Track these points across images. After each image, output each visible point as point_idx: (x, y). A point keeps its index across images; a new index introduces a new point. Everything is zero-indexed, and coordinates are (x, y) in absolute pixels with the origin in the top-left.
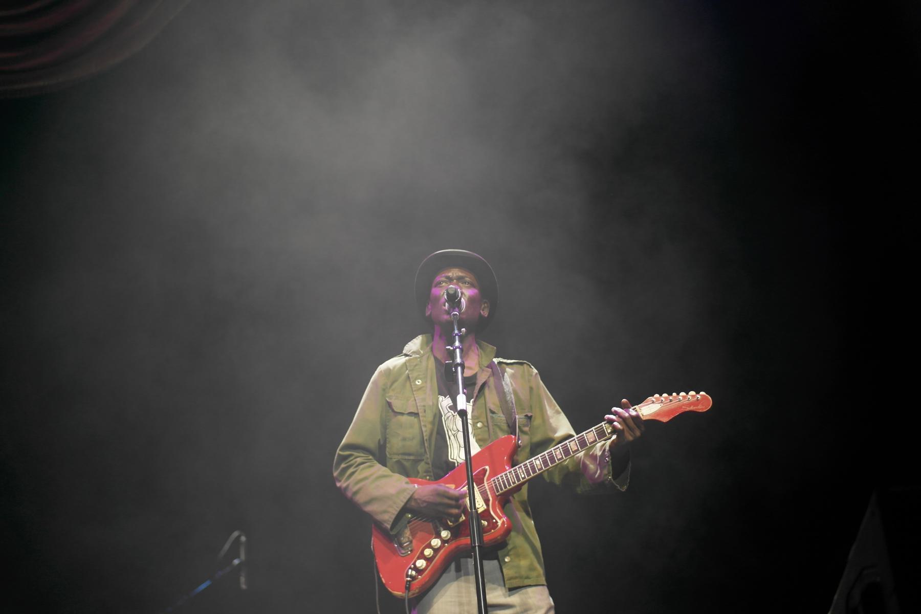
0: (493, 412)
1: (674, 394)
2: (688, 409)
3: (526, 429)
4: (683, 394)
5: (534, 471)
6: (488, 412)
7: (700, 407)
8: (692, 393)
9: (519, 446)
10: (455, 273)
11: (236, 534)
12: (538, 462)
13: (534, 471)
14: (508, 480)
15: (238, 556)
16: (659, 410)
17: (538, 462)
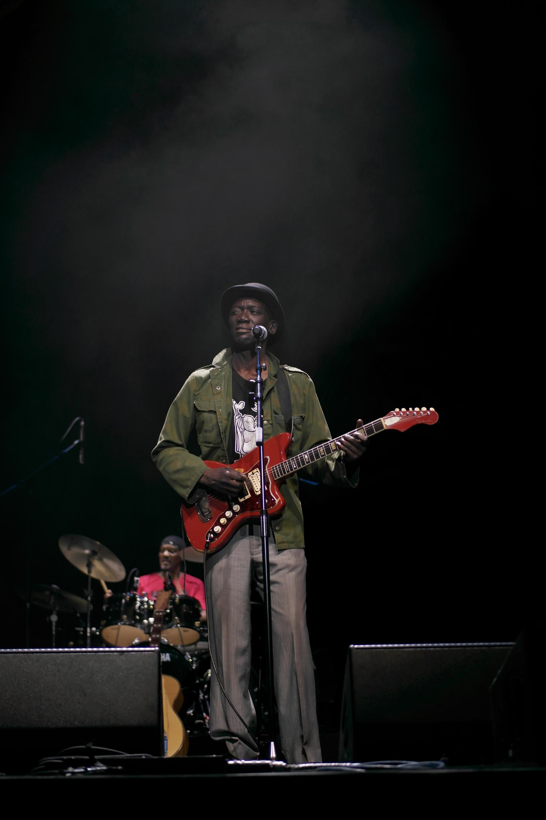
0: (276, 413)
1: (411, 409)
2: (420, 422)
4: (417, 409)
5: (303, 464)
6: (273, 412)
7: (429, 421)
8: (424, 409)
9: (293, 442)
11: (77, 419)
12: (306, 457)
13: (303, 464)
15: (78, 438)
16: (398, 422)
17: (306, 457)
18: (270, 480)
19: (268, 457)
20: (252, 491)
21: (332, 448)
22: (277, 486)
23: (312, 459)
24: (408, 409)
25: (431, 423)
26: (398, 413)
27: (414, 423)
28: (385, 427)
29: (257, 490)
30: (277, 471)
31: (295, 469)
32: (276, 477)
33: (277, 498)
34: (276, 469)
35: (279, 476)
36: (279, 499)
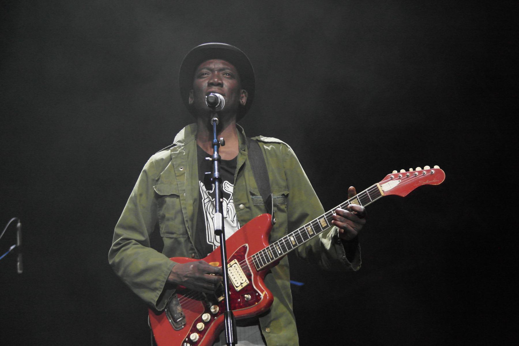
1: (411, 170)
3: (283, 207)
4: (418, 169)
5: (290, 248)
7: (434, 181)
8: (427, 168)
10: (217, 65)
12: (292, 239)
13: (290, 248)
14: (266, 256)
15: (15, 243)
17: (292, 239)
18: (251, 271)
19: (247, 245)
20: (231, 287)
21: (323, 227)
22: (261, 276)
23: (300, 241)
24: (407, 170)
25: (437, 182)
26: (396, 176)
27: (417, 186)
28: (383, 194)
29: (237, 285)
30: (259, 260)
31: (280, 254)
32: (258, 267)
33: (262, 291)
34: (258, 257)
35: (261, 265)
36: (264, 293)
